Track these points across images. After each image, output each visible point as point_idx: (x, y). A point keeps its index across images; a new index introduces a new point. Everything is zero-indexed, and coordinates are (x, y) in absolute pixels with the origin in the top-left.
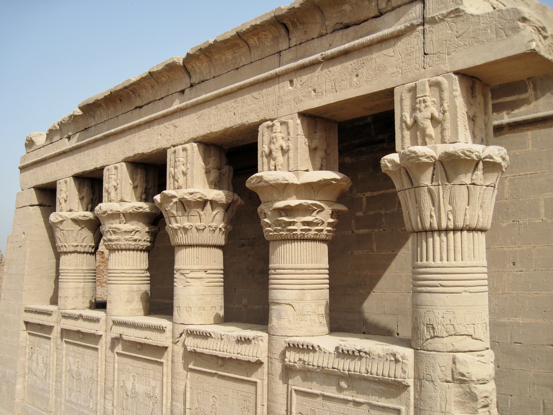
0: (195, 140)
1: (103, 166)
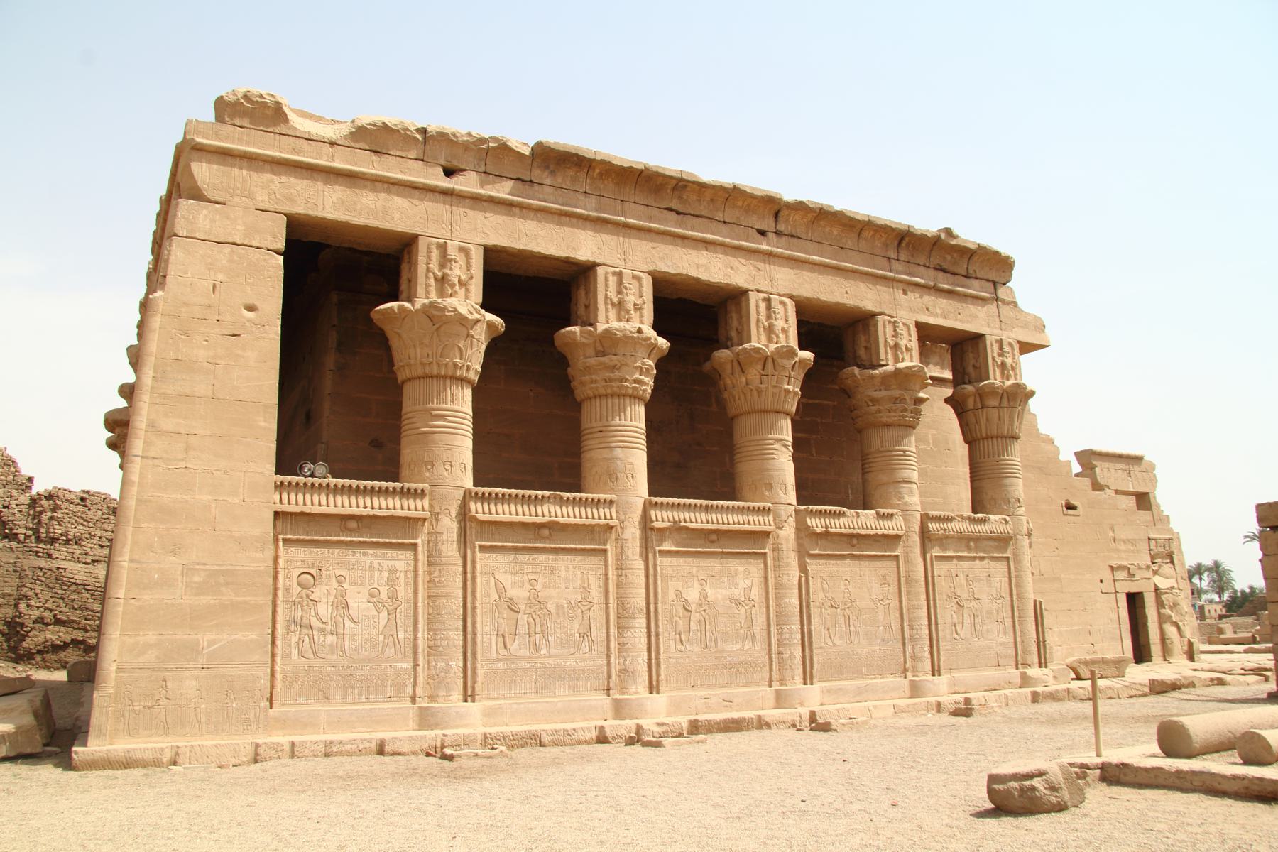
0: (791, 297)
1: (595, 262)
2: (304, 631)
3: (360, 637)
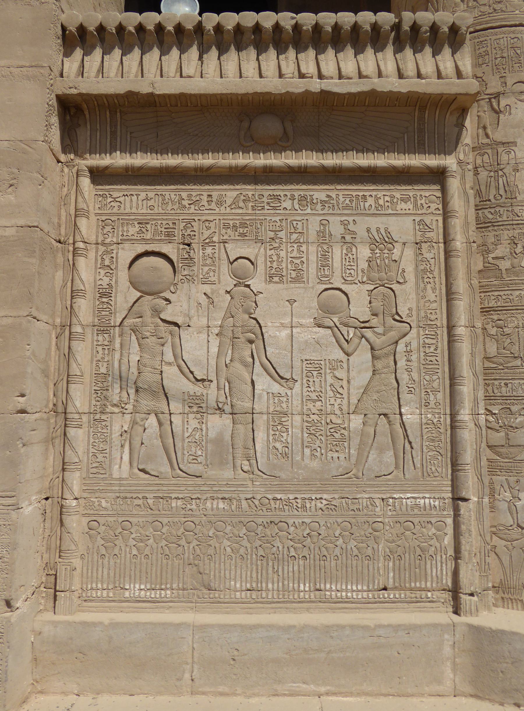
2: (146, 403)
3: (298, 419)
